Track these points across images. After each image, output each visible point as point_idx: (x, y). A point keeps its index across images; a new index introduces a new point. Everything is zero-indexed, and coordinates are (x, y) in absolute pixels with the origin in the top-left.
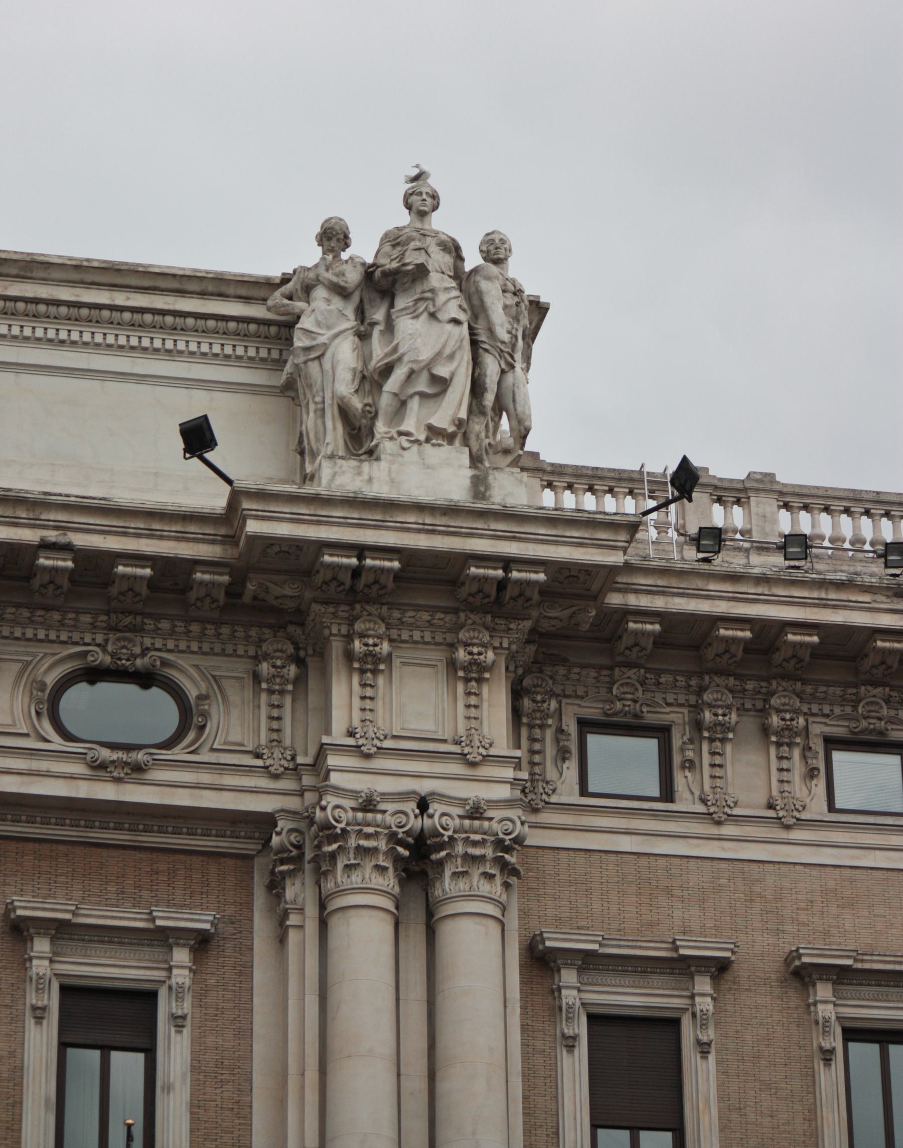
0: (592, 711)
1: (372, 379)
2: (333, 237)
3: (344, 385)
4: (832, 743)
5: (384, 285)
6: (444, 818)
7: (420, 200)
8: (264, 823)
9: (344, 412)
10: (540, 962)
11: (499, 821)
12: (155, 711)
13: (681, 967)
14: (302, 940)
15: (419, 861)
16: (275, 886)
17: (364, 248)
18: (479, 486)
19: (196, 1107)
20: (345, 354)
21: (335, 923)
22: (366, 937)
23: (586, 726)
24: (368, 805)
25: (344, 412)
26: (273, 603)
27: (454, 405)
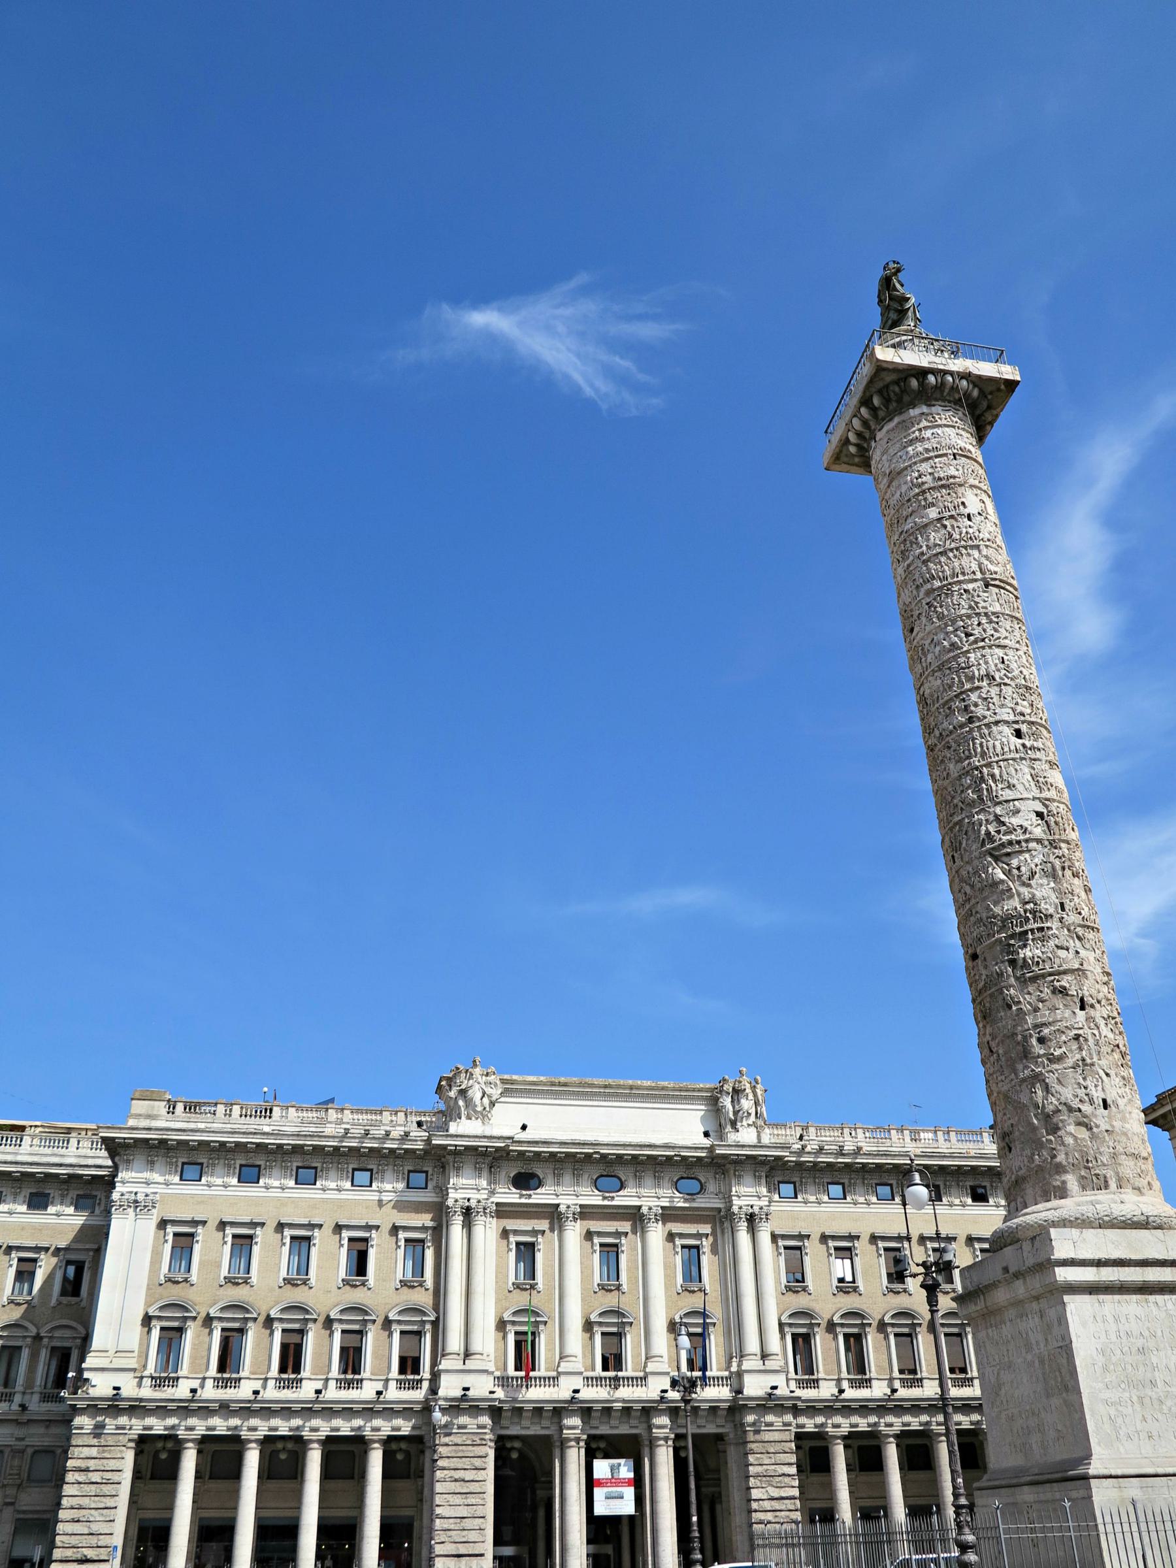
0: (780, 1179)
1: (736, 1113)
4: (828, 1183)
6: (756, 1210)
8: (719, 1210)
12: (694, 1186)
14: (728, 1235)
15: (751, 1219)
16: (722, 1223)
18: (759, 1137)
22: (743, 1237)
23: (779, 1182)
24: (740, 1208)
27: (752, 1118)
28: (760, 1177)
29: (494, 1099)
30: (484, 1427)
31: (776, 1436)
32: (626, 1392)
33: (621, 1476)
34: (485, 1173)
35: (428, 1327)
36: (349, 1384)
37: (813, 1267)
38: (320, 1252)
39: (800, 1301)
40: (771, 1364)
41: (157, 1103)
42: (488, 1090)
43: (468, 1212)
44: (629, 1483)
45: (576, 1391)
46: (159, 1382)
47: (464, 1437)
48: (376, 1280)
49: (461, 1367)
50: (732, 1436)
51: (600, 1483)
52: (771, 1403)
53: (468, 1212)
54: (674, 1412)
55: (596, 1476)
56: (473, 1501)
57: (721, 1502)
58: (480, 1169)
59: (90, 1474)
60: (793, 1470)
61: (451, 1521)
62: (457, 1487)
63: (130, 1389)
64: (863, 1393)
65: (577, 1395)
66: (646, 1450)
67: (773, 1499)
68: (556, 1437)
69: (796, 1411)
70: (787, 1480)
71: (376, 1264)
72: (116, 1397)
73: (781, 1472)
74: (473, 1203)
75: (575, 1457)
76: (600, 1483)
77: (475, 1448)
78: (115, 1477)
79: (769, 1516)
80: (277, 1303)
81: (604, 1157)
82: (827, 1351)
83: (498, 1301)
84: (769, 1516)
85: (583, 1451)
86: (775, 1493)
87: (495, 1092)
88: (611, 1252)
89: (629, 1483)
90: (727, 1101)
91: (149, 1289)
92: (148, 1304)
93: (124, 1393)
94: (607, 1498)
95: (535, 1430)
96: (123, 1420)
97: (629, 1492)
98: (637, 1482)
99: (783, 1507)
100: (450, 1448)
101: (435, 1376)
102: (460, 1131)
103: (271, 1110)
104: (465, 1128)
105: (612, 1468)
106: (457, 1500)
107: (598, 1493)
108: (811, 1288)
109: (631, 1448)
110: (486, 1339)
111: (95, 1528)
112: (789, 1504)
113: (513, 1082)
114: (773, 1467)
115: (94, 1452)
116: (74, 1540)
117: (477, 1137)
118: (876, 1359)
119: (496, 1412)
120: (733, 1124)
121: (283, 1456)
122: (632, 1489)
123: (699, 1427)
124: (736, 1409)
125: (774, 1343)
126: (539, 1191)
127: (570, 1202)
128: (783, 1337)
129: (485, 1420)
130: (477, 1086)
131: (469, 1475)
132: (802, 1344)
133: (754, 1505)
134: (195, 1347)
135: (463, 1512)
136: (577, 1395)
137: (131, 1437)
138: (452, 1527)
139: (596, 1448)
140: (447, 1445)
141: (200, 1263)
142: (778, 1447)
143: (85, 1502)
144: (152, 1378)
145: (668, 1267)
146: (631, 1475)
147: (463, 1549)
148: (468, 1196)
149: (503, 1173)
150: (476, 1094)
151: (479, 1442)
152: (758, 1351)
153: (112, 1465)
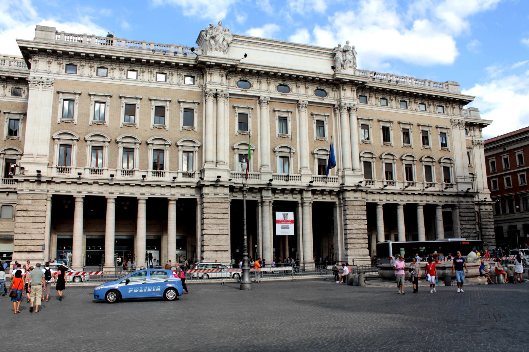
1: (344, 61)
2: (339, 46)
3: (342, 62)
5: (345, 51)
6: (352, 105)
7: (347, 43)
8: (334, 105)
9: (341, 64)
10: (358, 119)
11: (356, 106)
13: (369, 120)
15: (349, 109)
17: (342, 47)
18: (354, 73)
19: (329, 132)
20: (341, 58)
21: (342, 116)
22: (345, 116)
25: (341, 64)
26: (337, 83)
28: (354, 91)
29: (229, 42)
31: (359, 203)
32: (291, 182)
33: (288, 219)
34: (224, 78)
35: (197, 148)
36: (159, 174)
37: (373, 134)
38: (140, 112)
39: (368, 149)
40: (357, 173)
41: (49, 33)
42: (226, 38)
43: (216, 96)
44: (291, 222)
45: (271, 180)
46: (61, 170)
47: (217, 199)
48: (170, 126)
49: (215, 167)
50: (337, 203)
51: (279, 222)
52: (357, 189)
53: (216, 96)
54: (314, 192)
56: (222, 228)
58: (222, 76)
59: (29, 212)
60: (365, 217)
63: (46, 172)
64: (393, 187)
65: (271, 182)
66: (300, 208)
67: (356, 229)
68: (259, 201)
69: (366, 192)
70: (362, 221)
71: (170, 119)
72: (39, 176)
73: (360, 218)
74: (219, 92)
75: (268, 210)
76: (279, 222)
78: (43, 214)
79: (354, 236)
80: (120, 135)
81: (283, 75)
82: (378, 170)
83: (230, 139)
84: (354, 236)
85: (271, 208)
86: (358, 227)
87: (229, 39)
88: (283, 120)
89: (291, 222)
90: (339, 55)
91: (52, 125)
92: (52, 133)
93: (42, 174)
96: (44, 186)
97: (292, 226)
98: (295, 222)
99: (360, 233)
100: (211, 204)
101: (202, 171)
102: (212, 55)
103: (112, 41)
104: (214, 54)
105: (284, 215)
106: (215, 227)
107: (278, 226)
108: (372, 143)
110: (225, 155)
111: (34, 237)
112: (362, 231)
113: (237, 36)
114: (357, 216)
115: (30, 202)
116: (24, 243)
117: (221, 58)
118: (398, 174)
119: (232, 189)
120: (342, 66)
121: (125, 208)
122: (293, 224)
124: (341, 191)
125: (357, 164)
126: (250, 89)
127: (265, 95)
128: (360, 161)
129: (227, 191)
130: (221, 35)
131: (220, 216)
132: (368, 166)
133: (348, 232)
134: (78, 154)
136: (271, 182)
137: (48, 196)
138: (212, 239)
141: (79, 114)
142: (358, 208)
143: (28, 225)
144: (57, 168)
145: (310, 129)
146: (293, 219)
148: (217, 88)
149: (233, 80)
150: (220, 38)
152: (351, 168)
153: (40, 208)
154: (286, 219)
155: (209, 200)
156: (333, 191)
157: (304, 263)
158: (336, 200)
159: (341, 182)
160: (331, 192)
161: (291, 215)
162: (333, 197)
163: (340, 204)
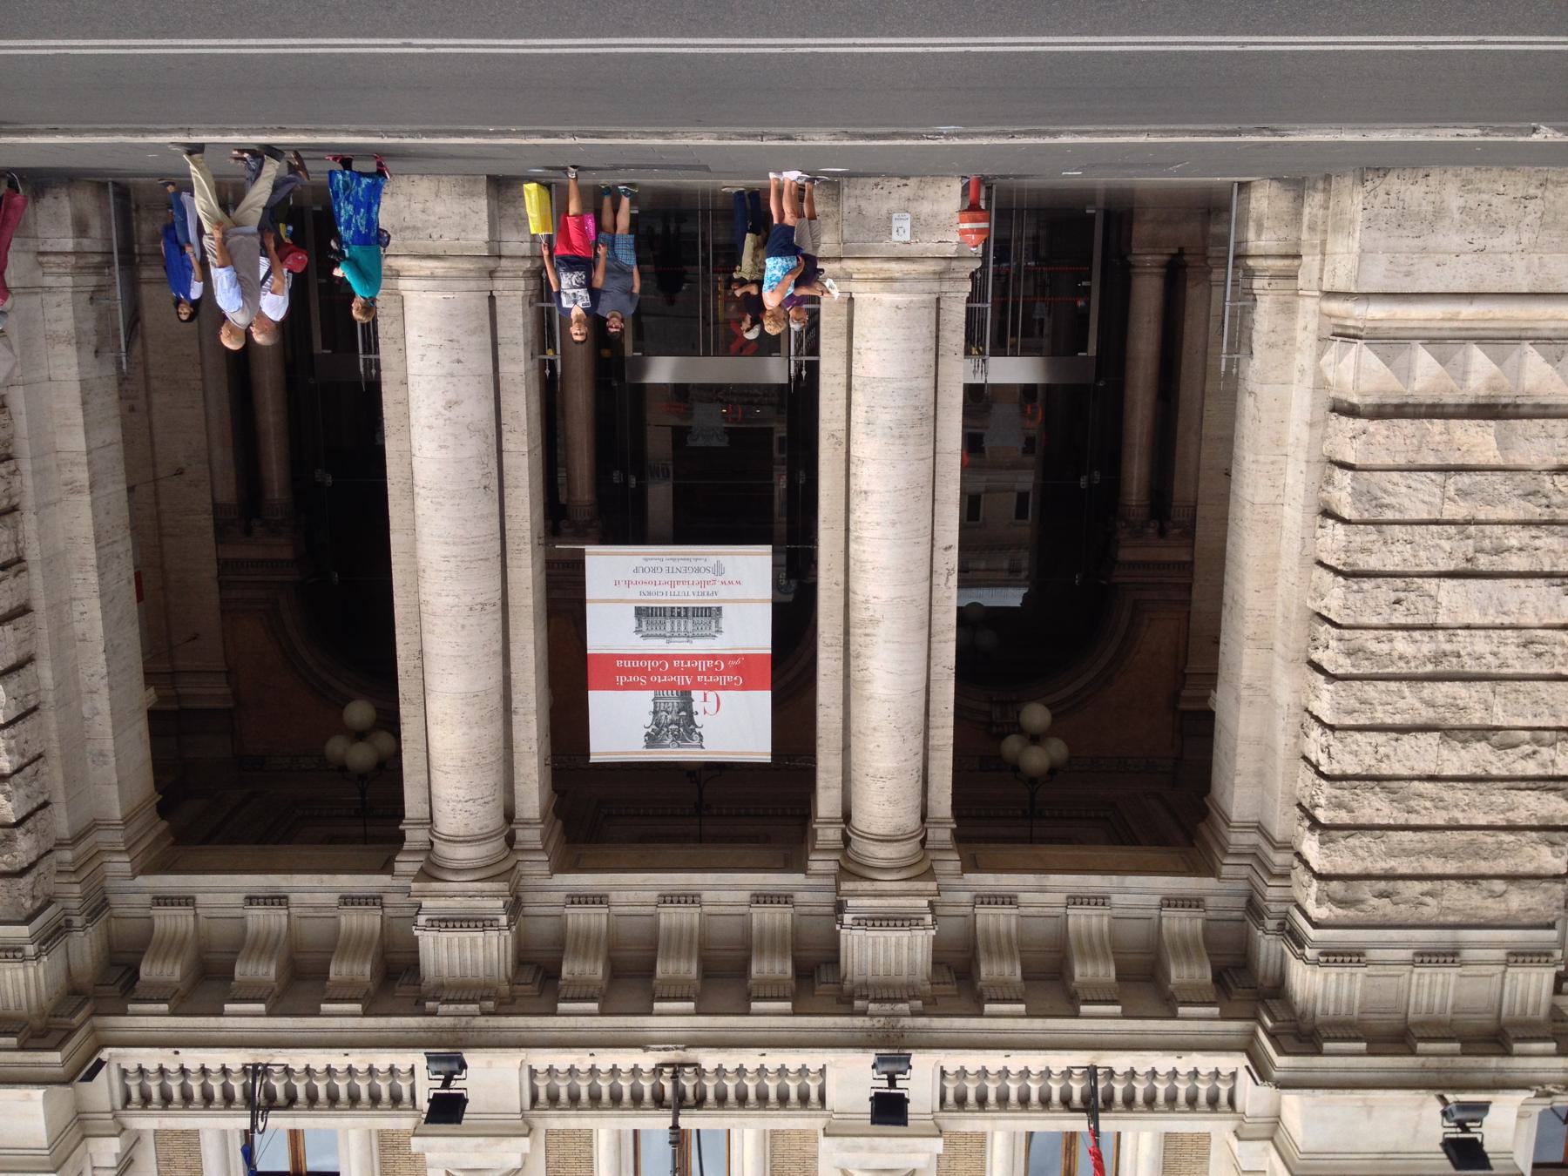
30: (1333, 956)
47: (1431, 909)
50: (120, 865)
51: (739, 671)
54: (396, 979)
55: (768, 694)
56: (1401, 643)
57: (217, 507)
61: (1518, 563)
62: (1474, 703)
66: (531, 797)
76: (739, 671)
77: (1379, 866)
85: (827, 802)
94: (710, 614)
95: (1038, 896)
97: (608, 630)
98: (570, 671)
100: (1502, 866)
105: (686, 727)
106: (1478, 650)
107: (750, 630)
109: (604, 810)
123: (278, 899)
131: (1424, 754)
135: (1454, 601)
138: (1515, 538)
139: (763, 808)
140: (1512, 878)
146: (600, 703)
147: (1478, 441)
151: (1365, 890)
154: (672, 701)
155: (1518, 900)
156: (182, 1002)
157: (492, 260)
158: (134, 890)
159: (102, 1092)
160: (209, 981)
161: (619, 727)
162: (172, 921)
163: (88, 866)
